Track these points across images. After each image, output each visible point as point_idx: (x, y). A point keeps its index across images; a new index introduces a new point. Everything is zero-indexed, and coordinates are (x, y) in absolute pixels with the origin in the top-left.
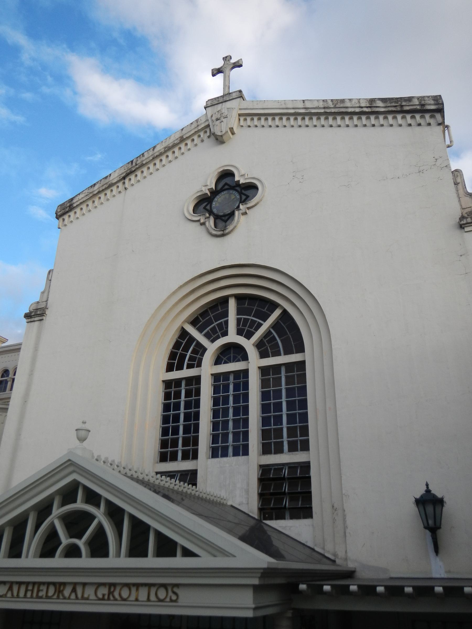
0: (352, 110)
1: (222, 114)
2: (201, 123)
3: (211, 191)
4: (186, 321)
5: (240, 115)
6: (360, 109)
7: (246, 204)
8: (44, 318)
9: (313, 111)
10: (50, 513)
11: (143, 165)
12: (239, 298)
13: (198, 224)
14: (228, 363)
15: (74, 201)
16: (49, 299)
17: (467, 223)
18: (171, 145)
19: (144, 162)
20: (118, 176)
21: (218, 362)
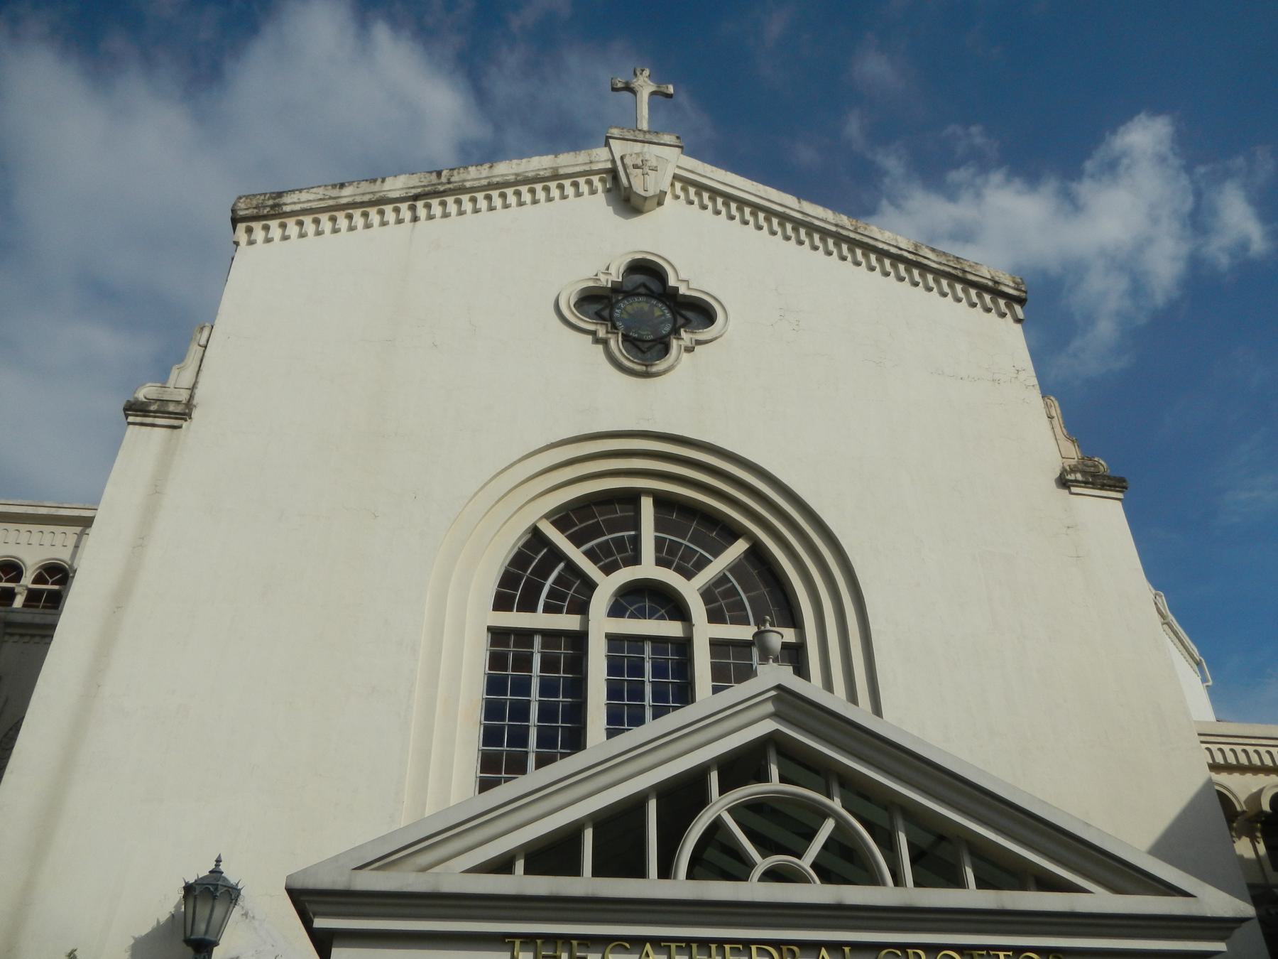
0: (886, 247)
1: (646, 160)
2: (597, 159)
3: (616, 289)
4: (547, 516)
5: (676, 177)
6: (897, 250)
7: (692, 332)
8: (185, 424)
9: (817, 223)
10: (702, 801)
11: (462, 190)
12: (663, 503)
13: (590, 338)
14: (640, 619)
15: (287, 199)
16: (199, 386)
17: (1076, 481)
18: (530, 175)
19: (468, 184)
20: (402, 189)
21: (616, 611)
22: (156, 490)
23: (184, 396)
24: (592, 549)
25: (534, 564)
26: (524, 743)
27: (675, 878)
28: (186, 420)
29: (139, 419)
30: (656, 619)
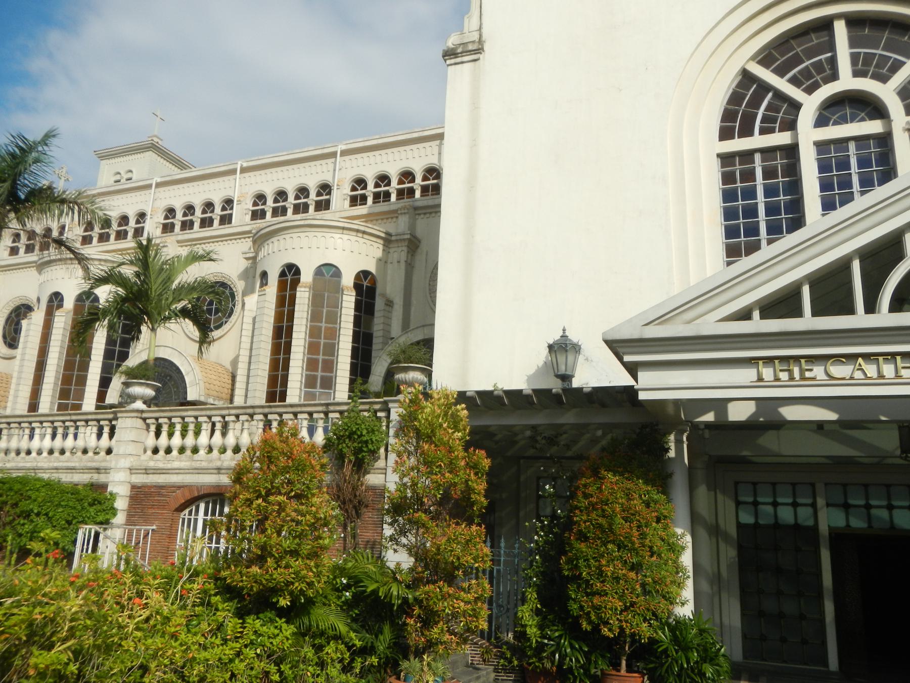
4: (753, 58)
8: (481, 56)
16: (484, 26)
21: (821, 121)
22: (475, 106)
23: (475, 37)
24: (794, 77)
25: (747, 99)
27: (879, 312)
28: (481, 53)
29: (453, 61)
30: (858, 122)
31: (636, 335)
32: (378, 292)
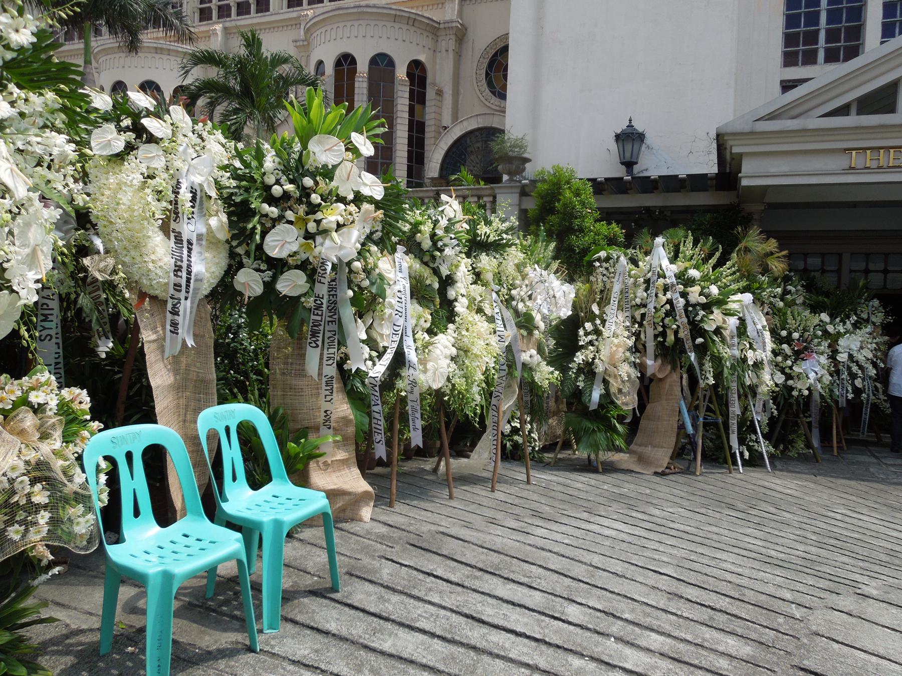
26: (817, 23)
31: (747, 128)
32: (429, 80)
